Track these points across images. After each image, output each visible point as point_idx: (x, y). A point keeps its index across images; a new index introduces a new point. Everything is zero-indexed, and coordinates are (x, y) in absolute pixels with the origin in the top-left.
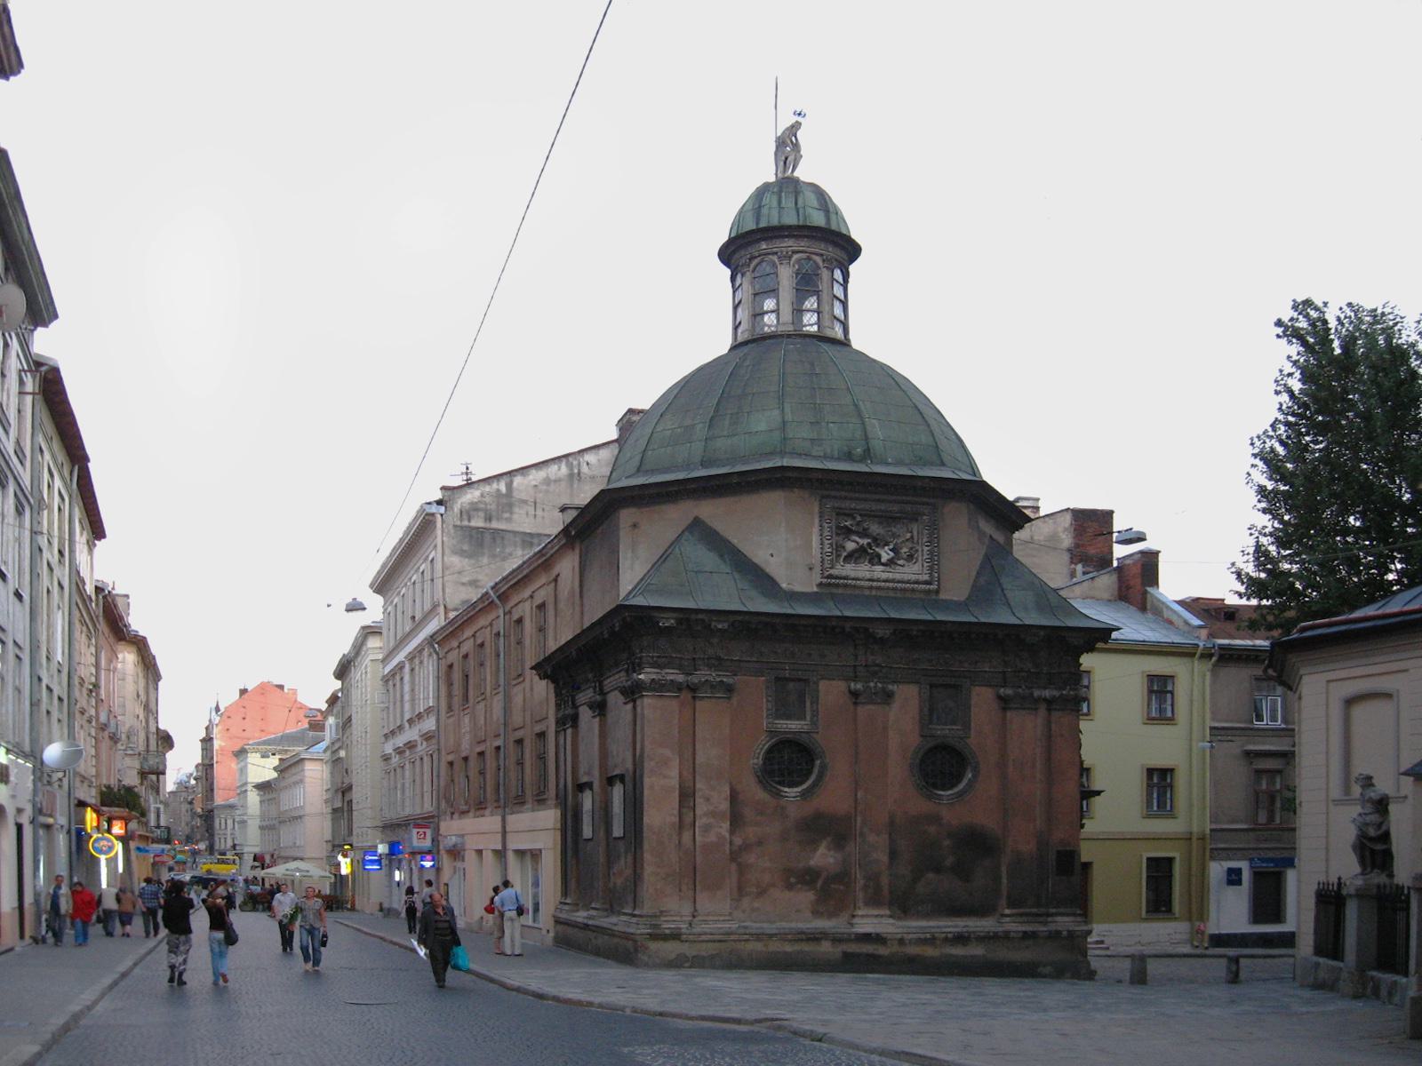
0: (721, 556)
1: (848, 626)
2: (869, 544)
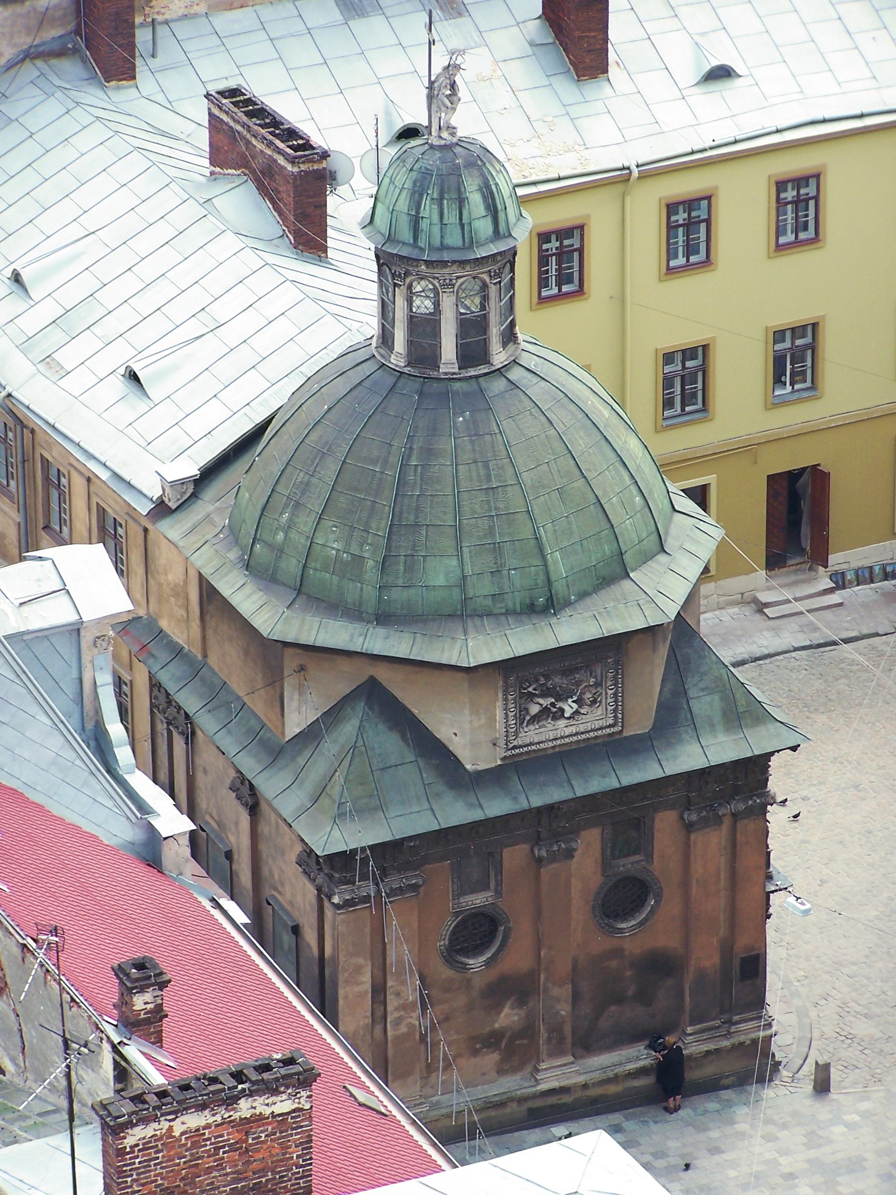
0: (404, 739)
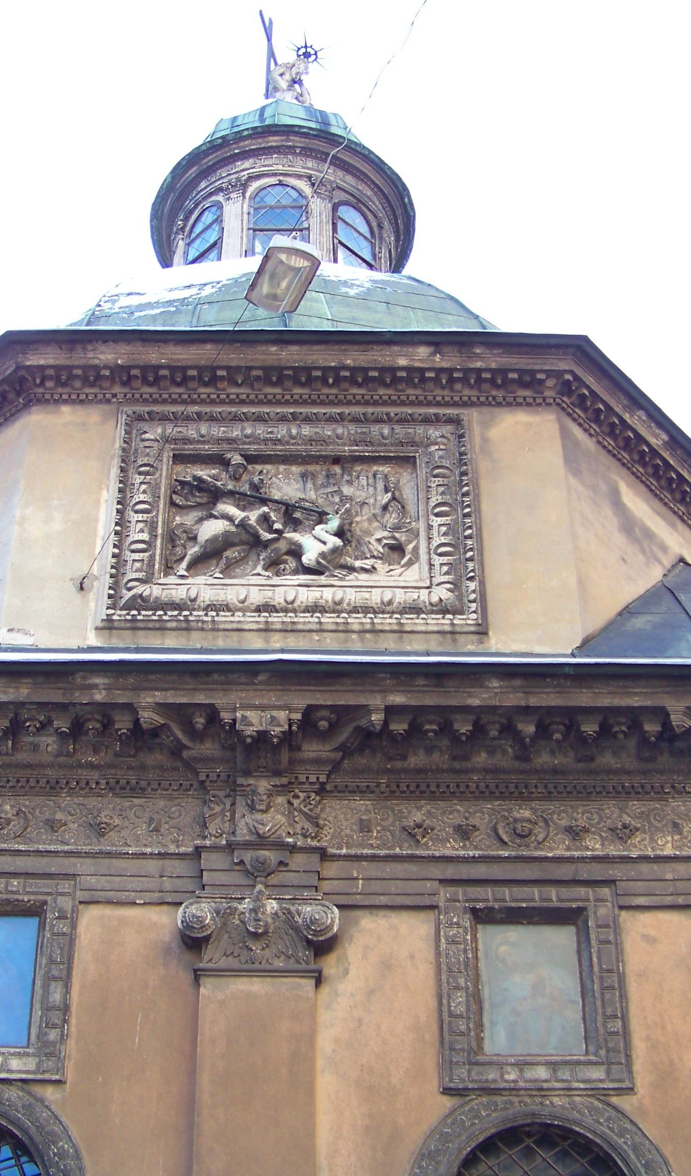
1: (149, 703)
2: (265, 519)
